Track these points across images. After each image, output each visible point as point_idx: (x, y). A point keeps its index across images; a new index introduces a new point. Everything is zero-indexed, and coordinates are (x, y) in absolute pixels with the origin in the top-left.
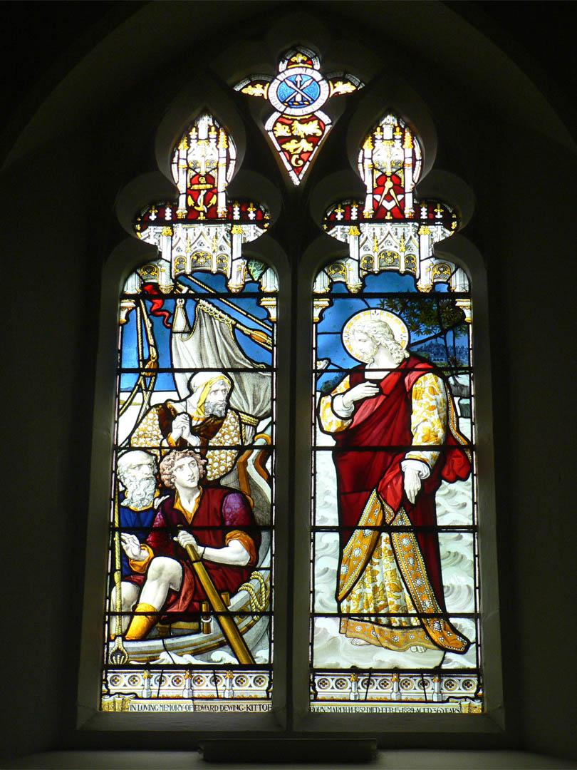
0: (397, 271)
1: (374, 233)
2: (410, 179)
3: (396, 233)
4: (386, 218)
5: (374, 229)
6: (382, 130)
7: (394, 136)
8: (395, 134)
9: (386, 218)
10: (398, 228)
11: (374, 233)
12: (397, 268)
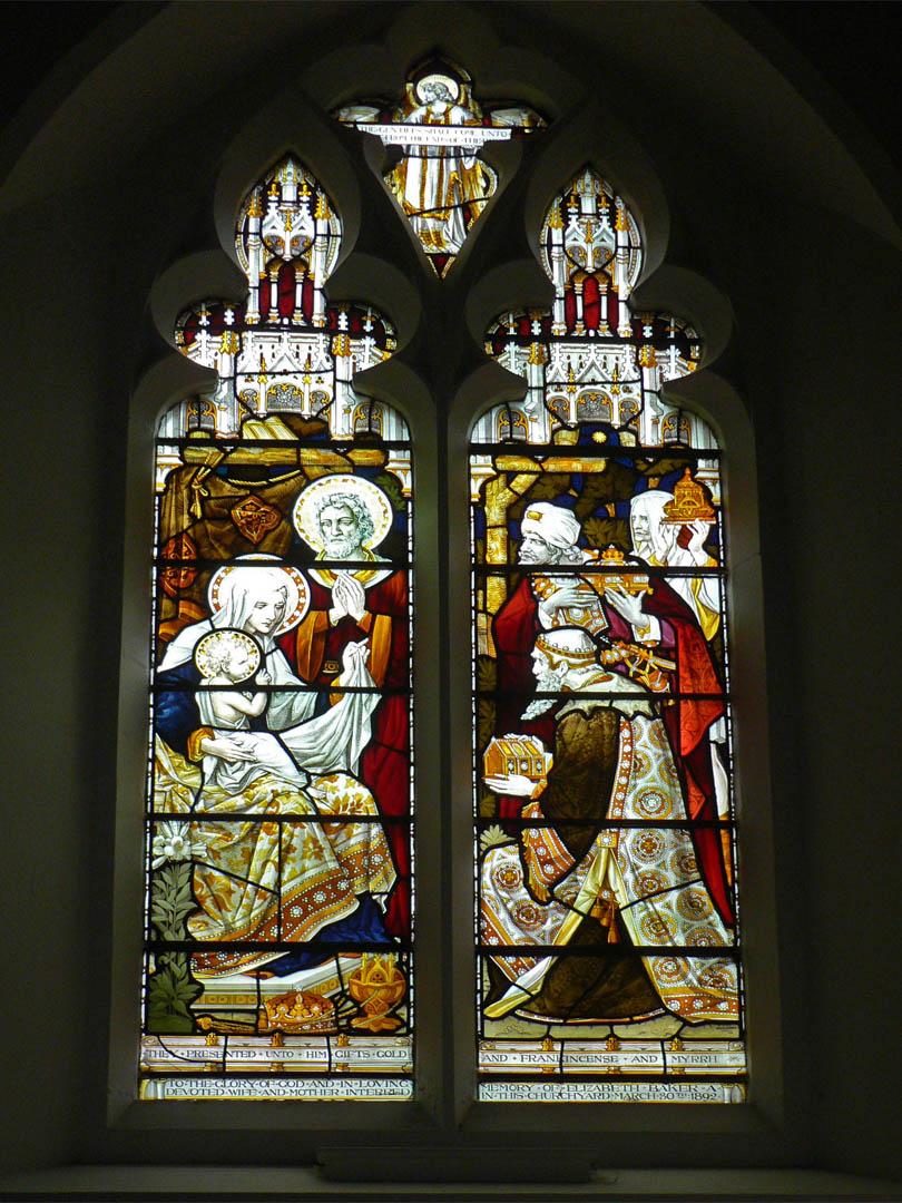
0: (299, 415)
1: (262, 354)
2: (320, 268)
3: (297, 353)
4: (201, 323)
5: (261, 347)
6: (279, 188)
7: (298, 196)
8: (300, 193)
9: (201, 323)
10: (263, 344)
11: (262, 354)
12: (297, 410)
